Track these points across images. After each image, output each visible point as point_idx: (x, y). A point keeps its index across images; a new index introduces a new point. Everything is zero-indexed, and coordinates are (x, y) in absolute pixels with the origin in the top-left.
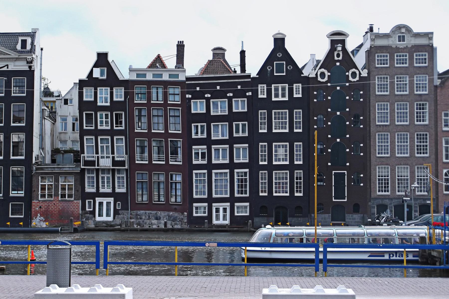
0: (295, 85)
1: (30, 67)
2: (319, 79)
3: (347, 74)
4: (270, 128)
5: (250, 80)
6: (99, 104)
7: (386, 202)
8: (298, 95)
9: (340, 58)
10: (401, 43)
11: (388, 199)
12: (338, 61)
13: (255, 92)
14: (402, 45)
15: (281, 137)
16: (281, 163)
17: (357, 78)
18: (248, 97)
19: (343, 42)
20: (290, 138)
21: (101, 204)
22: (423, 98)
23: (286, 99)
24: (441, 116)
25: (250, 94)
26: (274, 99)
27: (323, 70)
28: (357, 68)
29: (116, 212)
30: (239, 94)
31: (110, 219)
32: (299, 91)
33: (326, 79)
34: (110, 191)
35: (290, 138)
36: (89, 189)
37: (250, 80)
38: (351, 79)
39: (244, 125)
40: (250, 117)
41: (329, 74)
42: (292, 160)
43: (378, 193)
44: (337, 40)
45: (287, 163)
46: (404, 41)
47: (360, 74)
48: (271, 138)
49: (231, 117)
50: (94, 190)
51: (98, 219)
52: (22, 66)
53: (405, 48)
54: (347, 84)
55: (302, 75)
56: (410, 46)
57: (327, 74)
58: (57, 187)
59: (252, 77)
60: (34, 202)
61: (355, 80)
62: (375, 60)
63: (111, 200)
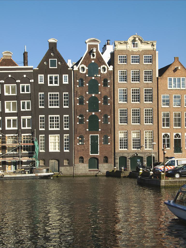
0: (64, 75)
2: (81, 71)
3: (99, 68)
5: (32, 71)
7: (125, 155)
8: (66, 82)
9: (95, 57)
10: (135, 48)
11: (127, 153)
12: (93, 59)
14: (135, 49)
15: (54, 111)
16: (55, 129)
17: (106, 72)
20: (61, 111)
22: (149, 85)
24: (161, 98)
25: (33, 81)
26: (49, 85)
27: (83, 65)
30: (25, 81)
32: (66, 80)
37: (32, 71)
38: (102, 72)
39: (28, 104)
41: (87, 68)
42: (62, 128)
43: (120, 149)
45: (58, 129)
46: (137, 47)
47: (108, 68)
48: (47, 112)
53: (137, 52)
54: (99, 76)
55: (69, 69)
56: (141, 50)
57: (86, 68)
59: (33, 69)
61: (105, 73)
62: (118, 59)
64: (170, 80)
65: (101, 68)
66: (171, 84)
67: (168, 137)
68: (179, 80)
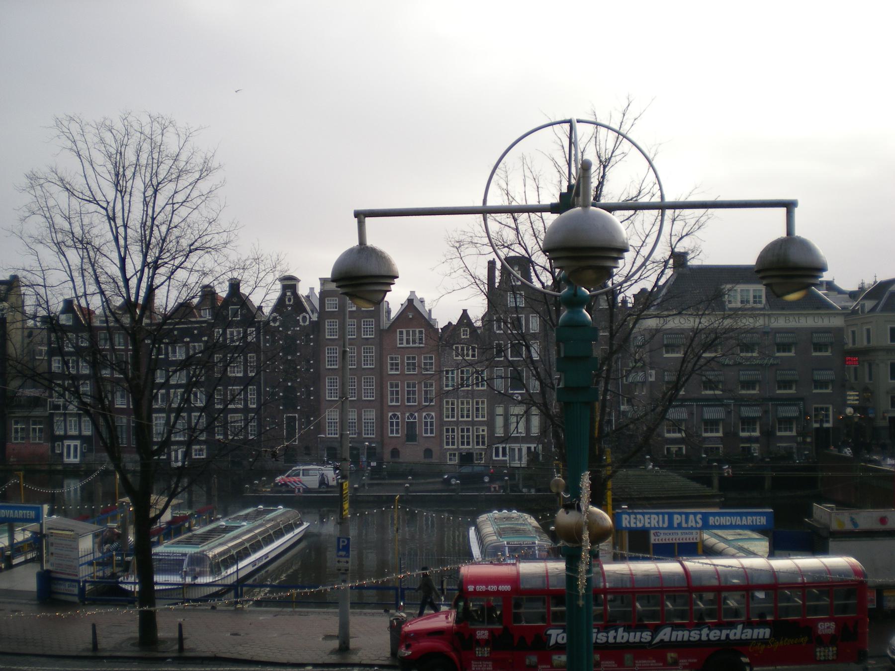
12: (289, 305)
17: (307, 323)
19: (293, 288)
21: (69, 446)
25: (205, 338)
27: (275, 314)
28: (307, 313)
29: (83, 455)
31: (77, 460)
33: (277, 324)
34: (77, 433)
38: (301, 323)
40: (207, 364)
44: (289, 284)
47: (310, 318)
50: (62, 433)
51: (66, 460)
58: (28, 430)
60: (8, 444)
63: (78, 443)
64: (401, 333)
65: (300, 318)
66: (401, 340)
67: (398, 418)
68: (414, 332)
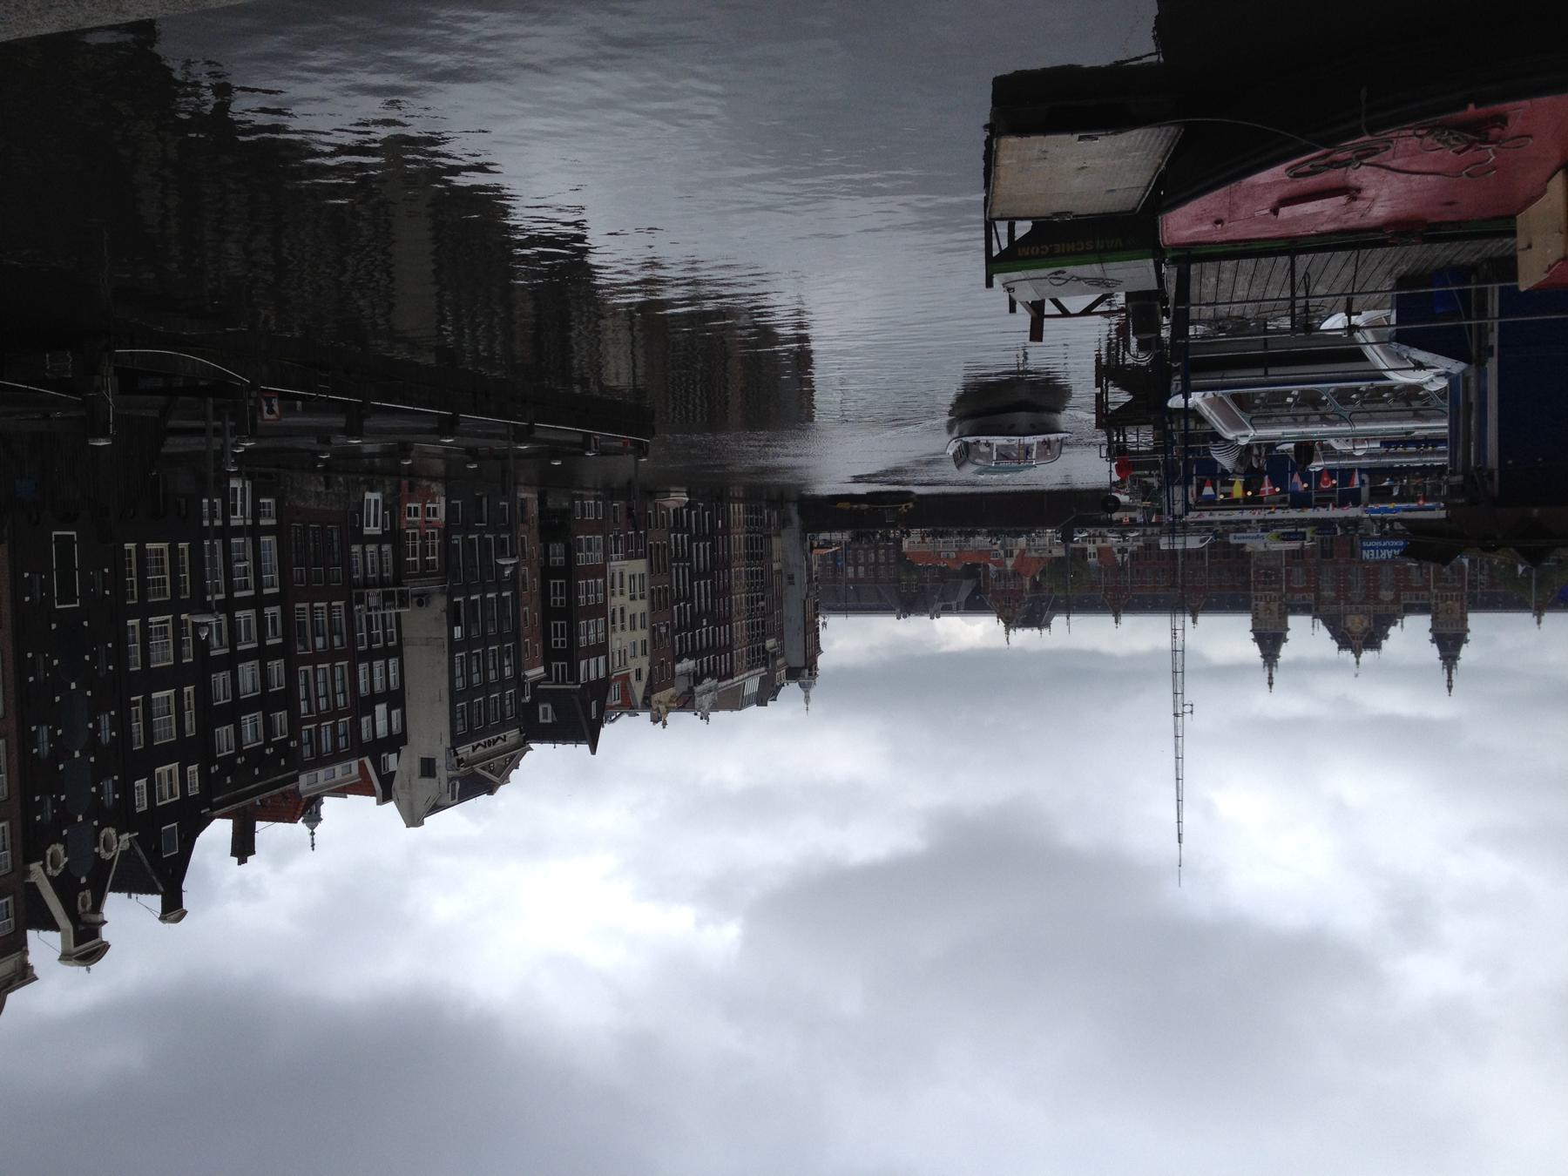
1: (456, 754)
2: (112, 831)
4: (179, 696)
6: (383, 706)
12: (84, 888)
13: (204, 774)
17: (49, 852)
18: (215, 761)
23: (158, 770)
25: (214, 769)
27: (108, 856)
28: (51, 878)
30: (228, 764)
35: (153, 679)
36: (386, 548)
38: (59, 848)
40: (210, 716)
47: (44, 867)
49: (234, 712)
52: (465, 751)
